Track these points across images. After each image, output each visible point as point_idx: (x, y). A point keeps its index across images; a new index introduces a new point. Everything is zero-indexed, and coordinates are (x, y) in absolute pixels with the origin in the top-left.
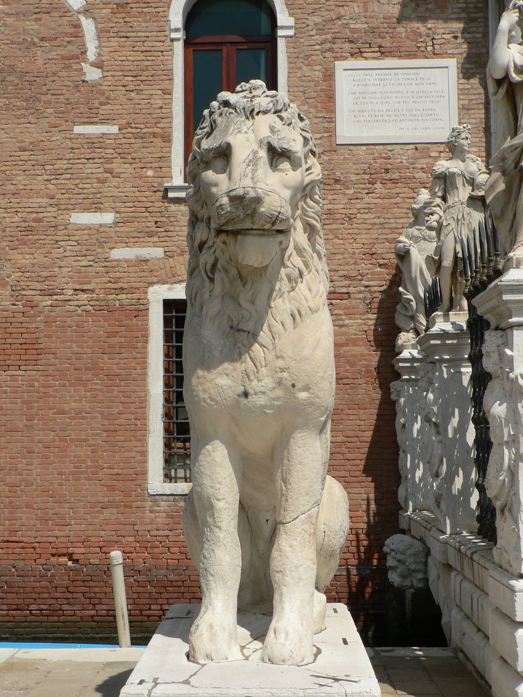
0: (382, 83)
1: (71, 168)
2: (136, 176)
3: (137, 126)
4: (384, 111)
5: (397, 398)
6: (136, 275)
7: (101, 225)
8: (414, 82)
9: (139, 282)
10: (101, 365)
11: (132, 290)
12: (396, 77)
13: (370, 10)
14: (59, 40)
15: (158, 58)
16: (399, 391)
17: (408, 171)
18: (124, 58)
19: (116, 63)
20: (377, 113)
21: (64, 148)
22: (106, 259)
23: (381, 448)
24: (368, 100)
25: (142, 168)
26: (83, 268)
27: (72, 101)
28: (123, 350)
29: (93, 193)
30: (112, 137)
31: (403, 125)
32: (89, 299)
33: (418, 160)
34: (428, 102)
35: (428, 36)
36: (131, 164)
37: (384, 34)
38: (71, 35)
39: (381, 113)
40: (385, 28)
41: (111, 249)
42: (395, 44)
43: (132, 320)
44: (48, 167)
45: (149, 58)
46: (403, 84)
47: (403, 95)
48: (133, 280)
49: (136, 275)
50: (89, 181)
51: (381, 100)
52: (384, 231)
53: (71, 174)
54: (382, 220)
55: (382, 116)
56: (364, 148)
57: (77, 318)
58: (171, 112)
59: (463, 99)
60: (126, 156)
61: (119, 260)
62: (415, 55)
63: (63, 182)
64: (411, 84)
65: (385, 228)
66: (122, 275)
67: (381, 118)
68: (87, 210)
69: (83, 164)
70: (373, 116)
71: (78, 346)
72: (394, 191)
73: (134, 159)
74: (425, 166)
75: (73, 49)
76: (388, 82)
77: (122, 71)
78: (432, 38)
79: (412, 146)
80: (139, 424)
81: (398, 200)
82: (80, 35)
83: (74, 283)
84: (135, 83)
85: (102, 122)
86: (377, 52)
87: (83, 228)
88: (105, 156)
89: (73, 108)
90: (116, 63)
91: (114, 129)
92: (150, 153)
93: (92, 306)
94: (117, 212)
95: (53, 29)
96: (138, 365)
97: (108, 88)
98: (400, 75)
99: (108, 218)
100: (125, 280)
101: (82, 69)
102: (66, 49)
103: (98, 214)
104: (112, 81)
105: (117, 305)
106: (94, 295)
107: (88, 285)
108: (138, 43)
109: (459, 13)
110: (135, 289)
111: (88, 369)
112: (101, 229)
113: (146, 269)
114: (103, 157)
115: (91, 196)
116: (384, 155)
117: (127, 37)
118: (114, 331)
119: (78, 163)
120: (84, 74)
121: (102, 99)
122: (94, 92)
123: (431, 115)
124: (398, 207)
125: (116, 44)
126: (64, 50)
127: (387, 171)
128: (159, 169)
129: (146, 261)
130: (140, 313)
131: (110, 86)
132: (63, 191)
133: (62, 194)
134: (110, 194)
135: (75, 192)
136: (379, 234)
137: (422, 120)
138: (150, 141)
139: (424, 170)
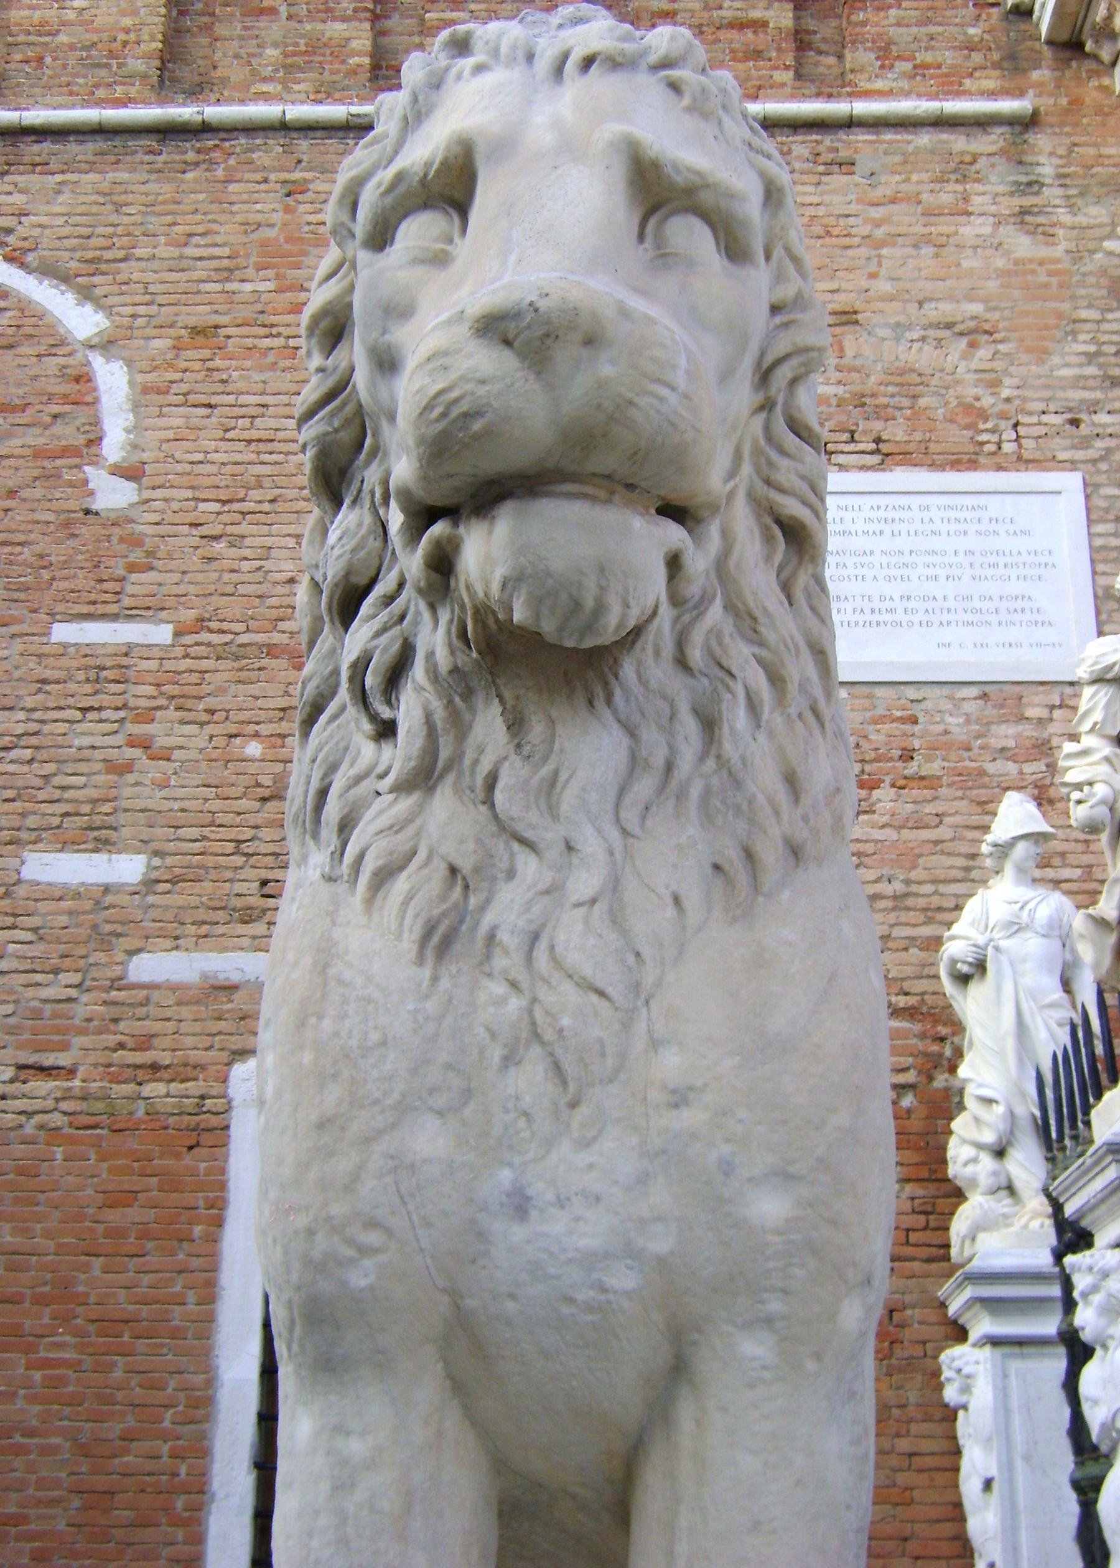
0: (887, 529)
1: (36, 734)
2: (214, 756)
3: (225, 626)
4: (897, 598)
5: (963, 1399)
6: (198, 1027)
7: (107, 889)
8: (972, 528)
9: (207, 1049)
10: (81, 1289)
11: (185, 1072)
12: (926, 515)
13: (850, 352)
14: (30, 411)
15: (291, 457)
16: (968, 1376)
17: (965, 754)
18: (199, 457)
19: (179, 468)
20: (876, 605)
21: (19, 680)
22: (118, 983)
23: (917, 1558)
24: (850, 571)
25: (231, 736)
26: (48, 1006)
27: (53, 559)
28: (150, 1245)
29: (95, 802)
30: (159, 654)
31: (947, 634)
32: (59, 1095)
33: (993, 727)
34: (1013, 578)
35: (1004, 416)
36: (202, 724)
37: (890, 410)
38: (66, 399)
39: (888, 604)
40: (893, 396)
42: (918, 436)
43: (178, 1156)
45: (266, 458)
46: (944, 532)
47: (946, 560)
48: (189, 1041)
49: (198, 1027)
50: (83, 767)
51: (886, 572)
52: (904, 917)
53: (36, 748)
54: (898, 887)
55: (890, 611)
57: (19, 1150)
59: (1104, 574)
60: (189, 704)
61: (153, 986)
62: (975, 462)
63: (12, 768)
64: (965, 533)
65: (909, 909)
66: (159, 1026)
67: (887, 617)
68: (67, 844)
69: (68, 721)
70: (867, 611)
71: (15, 1232)
72: (929, 809)
73: (212, 712)
74: (1012, 743)
75: (68, 433)
76: (903, 527)
77: (192, 487)
78: (1014, 421)
79: (974, 691)
80: (183, 1470)
81: (943, 832)
82: (89, 399)
83: (20, 1047)
84: (225, 518)
85: (130, 615)
86: (871, 453)
87: (57, 895)
88: (132, 702)
89: (53, 579)
90: (179, 468)
91: (162, 634)
92: (256, 698)
93: (65, 1113)
94: (156, 853)
95: (19, 385)
96: (191, 1293)
97: (150, 530)
98: (934, 509)
99: (128, 868)
100: (166, 1042)
101: (86, 482)
102: (47, 432)
103: (100, 858)
104: (163, 512)
105: (141, 1113)
106: (77, 1083)
107: (61, 1055)
108: (240, 421)
109: (1081, 365)
110: (195, 1067)
111: (41, 1300)
112: (109, 899)
113: (228, 1011)
114: (125, 706)
115: (86, 808)
116: (898, 714)
117: (209, 406)
118: (127, 1187)
119: (56, 721)
120: (92, 493)
121: (137, 556)
122: (115, 539)
123: (1023, 611)
124: (943, 853)
125: (180, 422)
126: (41, 435)
127: (907, 756)
128: (279, 742)
129: (231, 988)
130: (206, 1139)
131: (157, 524)
132: (10, 794)
133: (6, 800)
134: (139, 804)
135: (42, 795)
136: (892, 926)
137: (1000, 623)
138: (256, 666)
139: (1009, 754)
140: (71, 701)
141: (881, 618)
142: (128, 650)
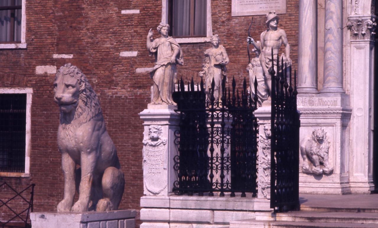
6: (146, 80)
30: (137, 15)
41: (136, 68)
44: (111, 30)
56: (244, 17)
57: (122, 100)
58: (161, 3)
68: (127, 50)
91: (137, 11)
103: (130, 52)
140: (125, 25)
141: (251, 3)
142: (133, 14)
